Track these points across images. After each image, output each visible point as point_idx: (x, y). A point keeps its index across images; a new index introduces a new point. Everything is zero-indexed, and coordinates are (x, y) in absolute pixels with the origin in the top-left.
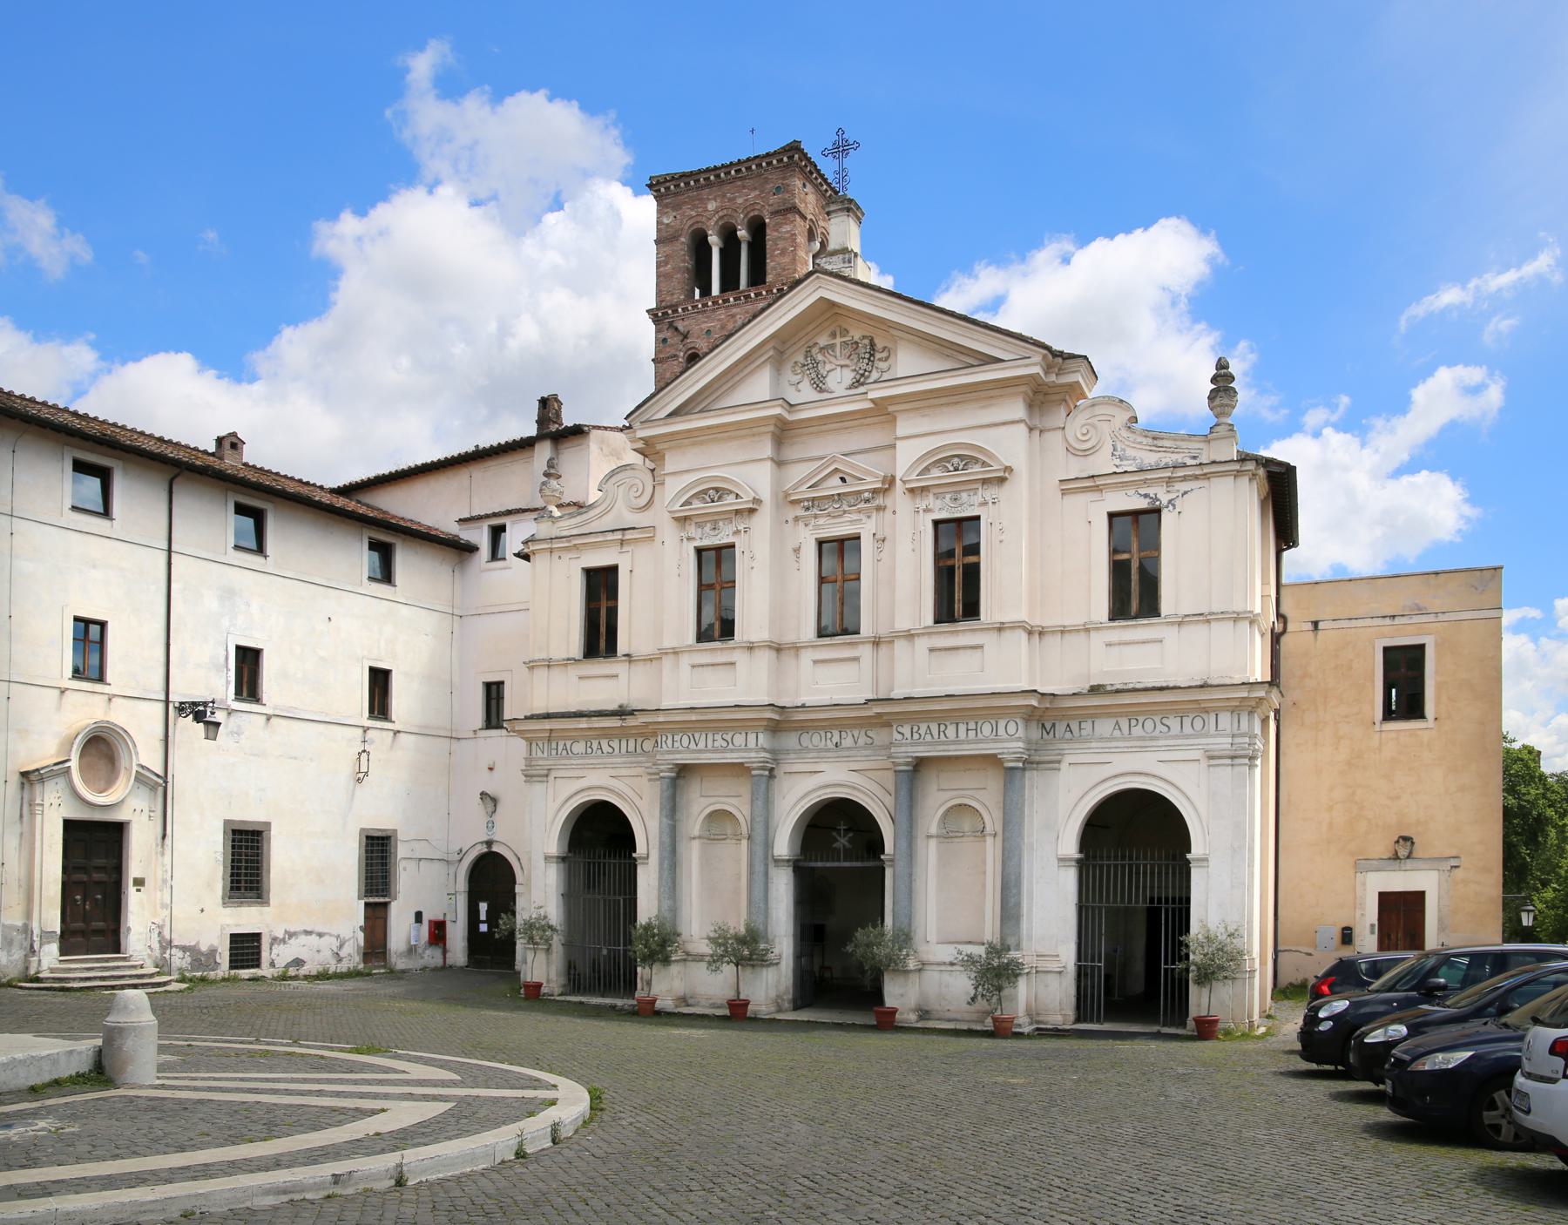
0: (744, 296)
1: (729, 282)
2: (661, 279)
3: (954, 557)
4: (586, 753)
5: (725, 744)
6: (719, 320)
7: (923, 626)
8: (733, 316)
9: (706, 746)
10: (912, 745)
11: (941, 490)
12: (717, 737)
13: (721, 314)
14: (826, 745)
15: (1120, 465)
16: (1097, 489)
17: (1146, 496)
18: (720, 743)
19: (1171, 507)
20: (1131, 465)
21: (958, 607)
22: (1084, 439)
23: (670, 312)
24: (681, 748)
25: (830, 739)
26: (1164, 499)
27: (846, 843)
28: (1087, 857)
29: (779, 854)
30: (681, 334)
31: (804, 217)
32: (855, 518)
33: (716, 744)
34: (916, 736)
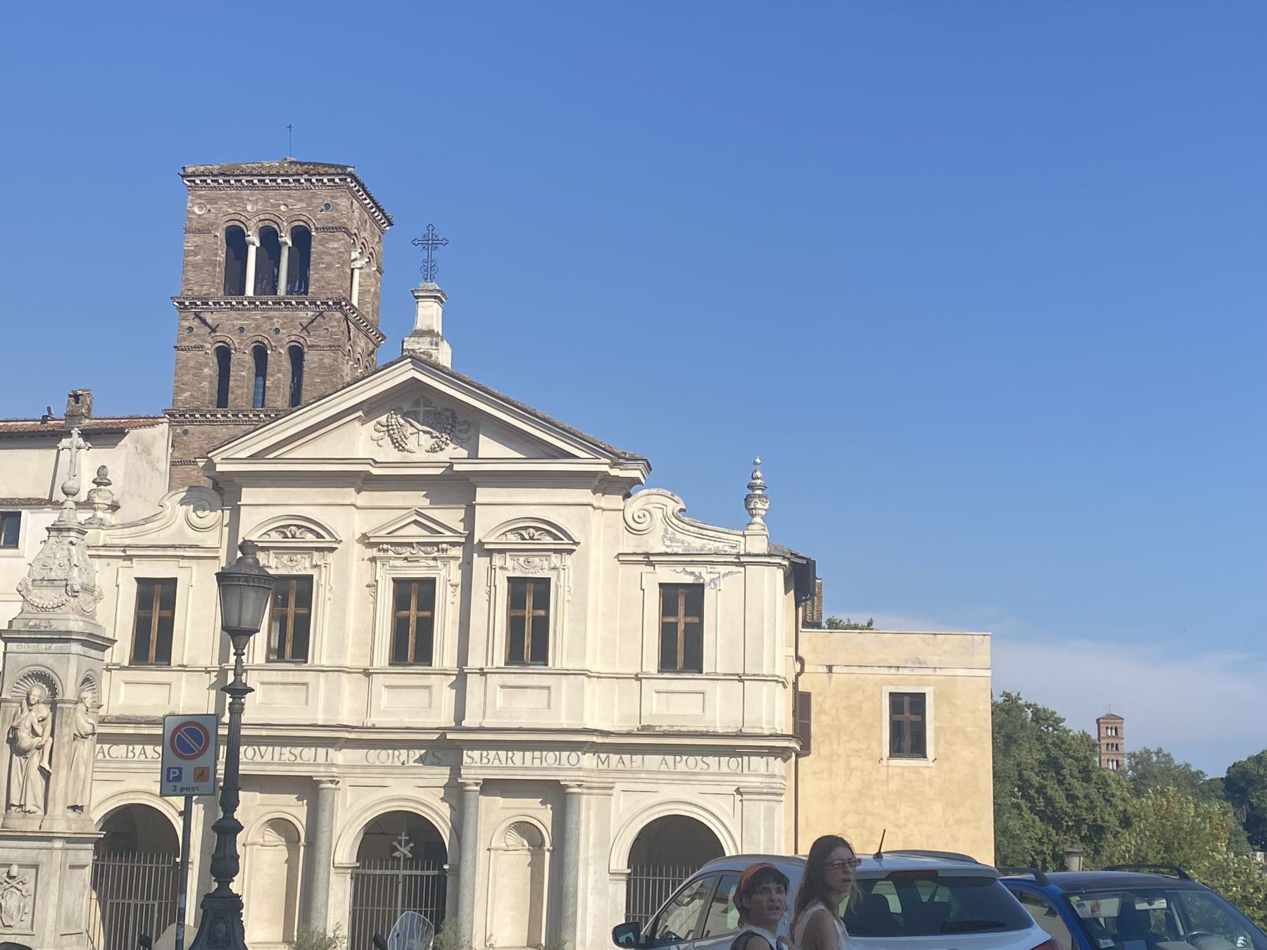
0: (284, 302)
1: (267, 282)
2: (189, 268)
3: (525, 609)
4: (127, 757)
5: (292, 758)
6: (254, 319)
7: (495, 665)
8: (270, 318)
9: (272, 759)
10: (481, 768)
12: (286, 750)
13: (258, 315)
14: (393, 762)
15: (671, 546)
16: (650, 564)
17: (692, 573)
19: (712, 585)
20: (680, 547)
21: (527, 653)
23: (199, 303)
25: (398, 757)
26: (707, 578)
27: (406, 852)
28: (635, 873)
29: (340, 861)
30: (209, 326)
31: (350, 235)
32: (431, 565)
33: (283, 757)
34: (485, 761)
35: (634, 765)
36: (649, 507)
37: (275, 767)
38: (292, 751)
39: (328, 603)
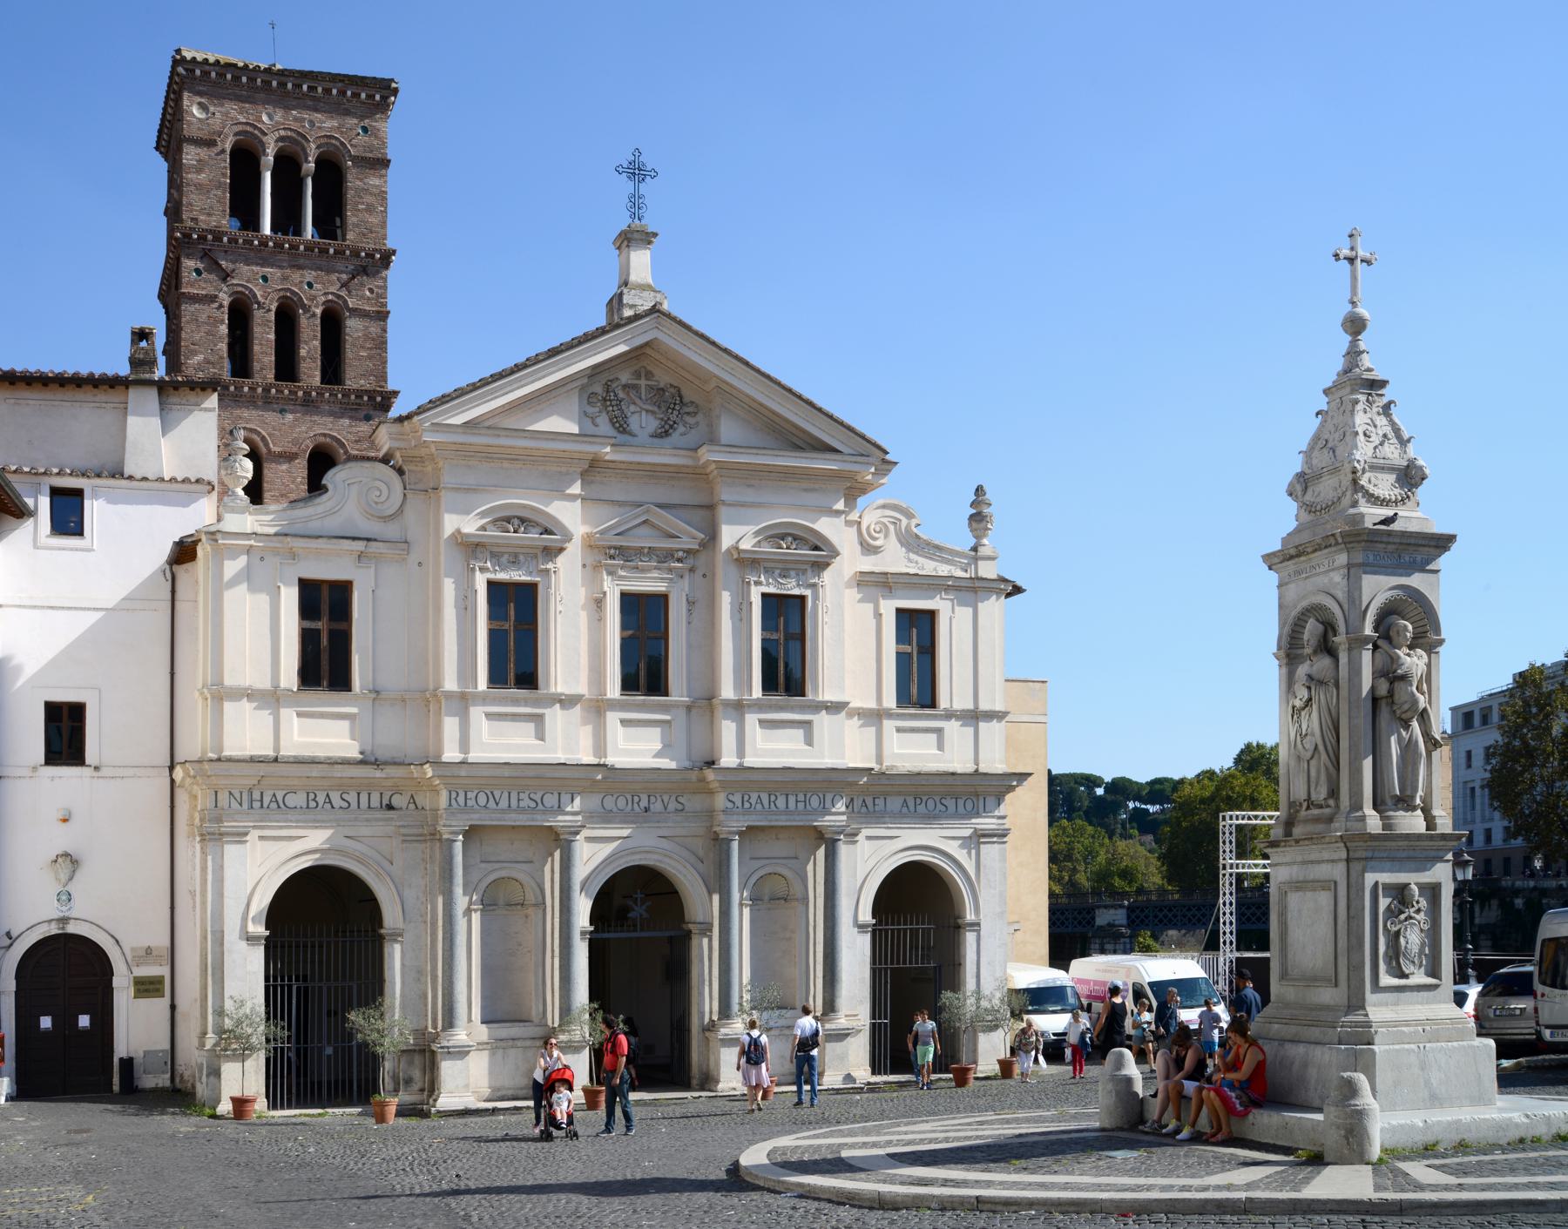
5: (533, 805)
11: (772, 565)
18: (526, 803)
22: (877, 535)
24: (476, 806)
35: (877, 808)
36: (885, 520)
37: (513, 815)
38: (532, 796)
39: (559, 616)
